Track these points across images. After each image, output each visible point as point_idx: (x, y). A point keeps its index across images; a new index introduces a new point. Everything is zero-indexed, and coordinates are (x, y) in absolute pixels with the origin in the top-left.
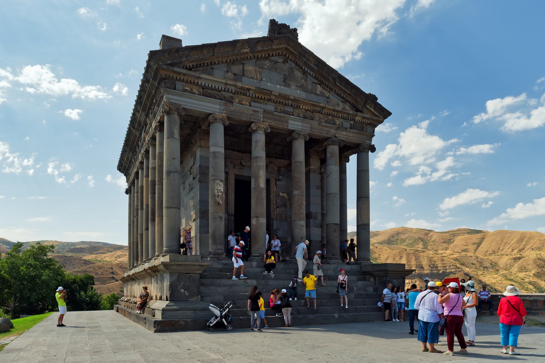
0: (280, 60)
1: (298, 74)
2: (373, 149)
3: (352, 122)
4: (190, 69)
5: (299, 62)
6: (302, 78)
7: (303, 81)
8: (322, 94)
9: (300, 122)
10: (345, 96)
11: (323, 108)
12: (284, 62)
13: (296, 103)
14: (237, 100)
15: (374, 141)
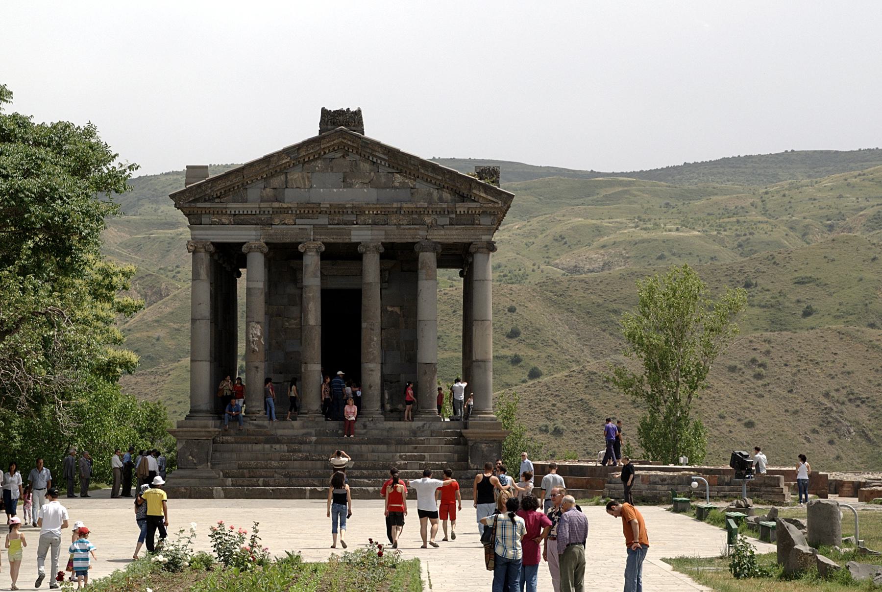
0: (338, 155)
1: (365, 166)
2: (491, 247)
3: (454, 216)
4: (219, 197)
5: (363, 153)
6: (371, 171)
7: (372, 174)
8: (403, 186)
9: (368, 229)
10: (438, 182)
11: (401, 208)
12: (343, 156)
13: (358, 211)
14: (277, 221)
15: (496, 237)
